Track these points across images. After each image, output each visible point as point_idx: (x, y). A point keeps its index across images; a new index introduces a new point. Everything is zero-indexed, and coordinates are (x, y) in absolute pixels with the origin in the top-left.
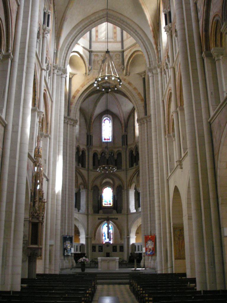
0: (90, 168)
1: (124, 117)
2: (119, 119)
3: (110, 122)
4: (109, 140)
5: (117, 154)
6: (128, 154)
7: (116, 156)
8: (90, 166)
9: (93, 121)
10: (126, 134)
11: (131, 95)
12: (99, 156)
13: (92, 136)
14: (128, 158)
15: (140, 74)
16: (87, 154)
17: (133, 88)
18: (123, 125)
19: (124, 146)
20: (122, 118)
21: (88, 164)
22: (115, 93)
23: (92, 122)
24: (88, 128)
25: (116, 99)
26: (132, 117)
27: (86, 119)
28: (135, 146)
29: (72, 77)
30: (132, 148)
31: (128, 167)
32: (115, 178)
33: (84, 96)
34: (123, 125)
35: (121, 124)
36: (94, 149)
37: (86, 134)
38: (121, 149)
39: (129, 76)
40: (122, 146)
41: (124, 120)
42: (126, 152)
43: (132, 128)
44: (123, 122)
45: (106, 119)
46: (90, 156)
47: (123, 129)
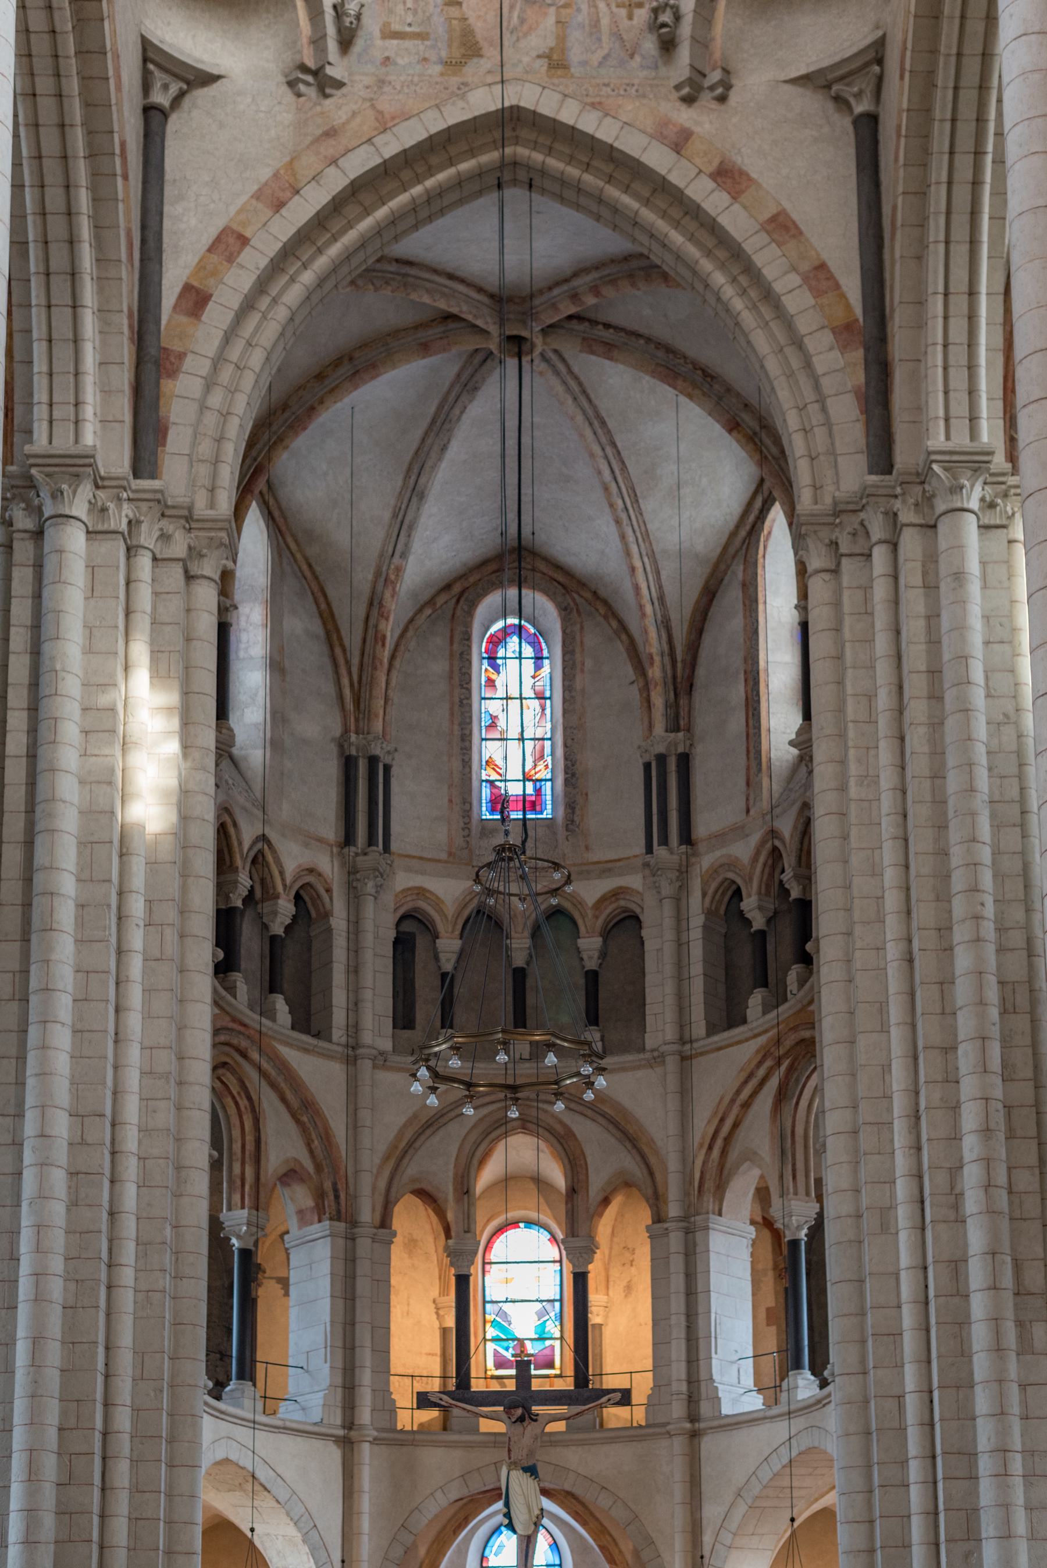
1: (662, 598)
3: (538, 659)
4: (531, 804)
7: (597, 942)
8: (368, 1021)
9: (390, 629)
10: (681, 749)
13: (387, 768)
14: (697, 950)
15: (828, 87)
16: (339, 922)
18: (655, 672)
19: (659, 851)
20: (649, 609)
22: (590, 345)
23: (390, 643)
24: (347, 692)
25: (597, 420)
26: (731, 596)
27: (328, 618)
28: (762, 843)
30: (731, 864)
31: (699, 1028)
32: (587, 1131)
33: (294, 295)
34: (655, 672)
35: (639, 663)
36: (403, 880)
37: (334, 749)
38: (634, 881)
39: (722, 99)
40: (649, 849)
41: (665, 624)
43: (738, 692)
44: (653, 644)
45: (506, 632)
46: (368, 939)
47: (658, 701)
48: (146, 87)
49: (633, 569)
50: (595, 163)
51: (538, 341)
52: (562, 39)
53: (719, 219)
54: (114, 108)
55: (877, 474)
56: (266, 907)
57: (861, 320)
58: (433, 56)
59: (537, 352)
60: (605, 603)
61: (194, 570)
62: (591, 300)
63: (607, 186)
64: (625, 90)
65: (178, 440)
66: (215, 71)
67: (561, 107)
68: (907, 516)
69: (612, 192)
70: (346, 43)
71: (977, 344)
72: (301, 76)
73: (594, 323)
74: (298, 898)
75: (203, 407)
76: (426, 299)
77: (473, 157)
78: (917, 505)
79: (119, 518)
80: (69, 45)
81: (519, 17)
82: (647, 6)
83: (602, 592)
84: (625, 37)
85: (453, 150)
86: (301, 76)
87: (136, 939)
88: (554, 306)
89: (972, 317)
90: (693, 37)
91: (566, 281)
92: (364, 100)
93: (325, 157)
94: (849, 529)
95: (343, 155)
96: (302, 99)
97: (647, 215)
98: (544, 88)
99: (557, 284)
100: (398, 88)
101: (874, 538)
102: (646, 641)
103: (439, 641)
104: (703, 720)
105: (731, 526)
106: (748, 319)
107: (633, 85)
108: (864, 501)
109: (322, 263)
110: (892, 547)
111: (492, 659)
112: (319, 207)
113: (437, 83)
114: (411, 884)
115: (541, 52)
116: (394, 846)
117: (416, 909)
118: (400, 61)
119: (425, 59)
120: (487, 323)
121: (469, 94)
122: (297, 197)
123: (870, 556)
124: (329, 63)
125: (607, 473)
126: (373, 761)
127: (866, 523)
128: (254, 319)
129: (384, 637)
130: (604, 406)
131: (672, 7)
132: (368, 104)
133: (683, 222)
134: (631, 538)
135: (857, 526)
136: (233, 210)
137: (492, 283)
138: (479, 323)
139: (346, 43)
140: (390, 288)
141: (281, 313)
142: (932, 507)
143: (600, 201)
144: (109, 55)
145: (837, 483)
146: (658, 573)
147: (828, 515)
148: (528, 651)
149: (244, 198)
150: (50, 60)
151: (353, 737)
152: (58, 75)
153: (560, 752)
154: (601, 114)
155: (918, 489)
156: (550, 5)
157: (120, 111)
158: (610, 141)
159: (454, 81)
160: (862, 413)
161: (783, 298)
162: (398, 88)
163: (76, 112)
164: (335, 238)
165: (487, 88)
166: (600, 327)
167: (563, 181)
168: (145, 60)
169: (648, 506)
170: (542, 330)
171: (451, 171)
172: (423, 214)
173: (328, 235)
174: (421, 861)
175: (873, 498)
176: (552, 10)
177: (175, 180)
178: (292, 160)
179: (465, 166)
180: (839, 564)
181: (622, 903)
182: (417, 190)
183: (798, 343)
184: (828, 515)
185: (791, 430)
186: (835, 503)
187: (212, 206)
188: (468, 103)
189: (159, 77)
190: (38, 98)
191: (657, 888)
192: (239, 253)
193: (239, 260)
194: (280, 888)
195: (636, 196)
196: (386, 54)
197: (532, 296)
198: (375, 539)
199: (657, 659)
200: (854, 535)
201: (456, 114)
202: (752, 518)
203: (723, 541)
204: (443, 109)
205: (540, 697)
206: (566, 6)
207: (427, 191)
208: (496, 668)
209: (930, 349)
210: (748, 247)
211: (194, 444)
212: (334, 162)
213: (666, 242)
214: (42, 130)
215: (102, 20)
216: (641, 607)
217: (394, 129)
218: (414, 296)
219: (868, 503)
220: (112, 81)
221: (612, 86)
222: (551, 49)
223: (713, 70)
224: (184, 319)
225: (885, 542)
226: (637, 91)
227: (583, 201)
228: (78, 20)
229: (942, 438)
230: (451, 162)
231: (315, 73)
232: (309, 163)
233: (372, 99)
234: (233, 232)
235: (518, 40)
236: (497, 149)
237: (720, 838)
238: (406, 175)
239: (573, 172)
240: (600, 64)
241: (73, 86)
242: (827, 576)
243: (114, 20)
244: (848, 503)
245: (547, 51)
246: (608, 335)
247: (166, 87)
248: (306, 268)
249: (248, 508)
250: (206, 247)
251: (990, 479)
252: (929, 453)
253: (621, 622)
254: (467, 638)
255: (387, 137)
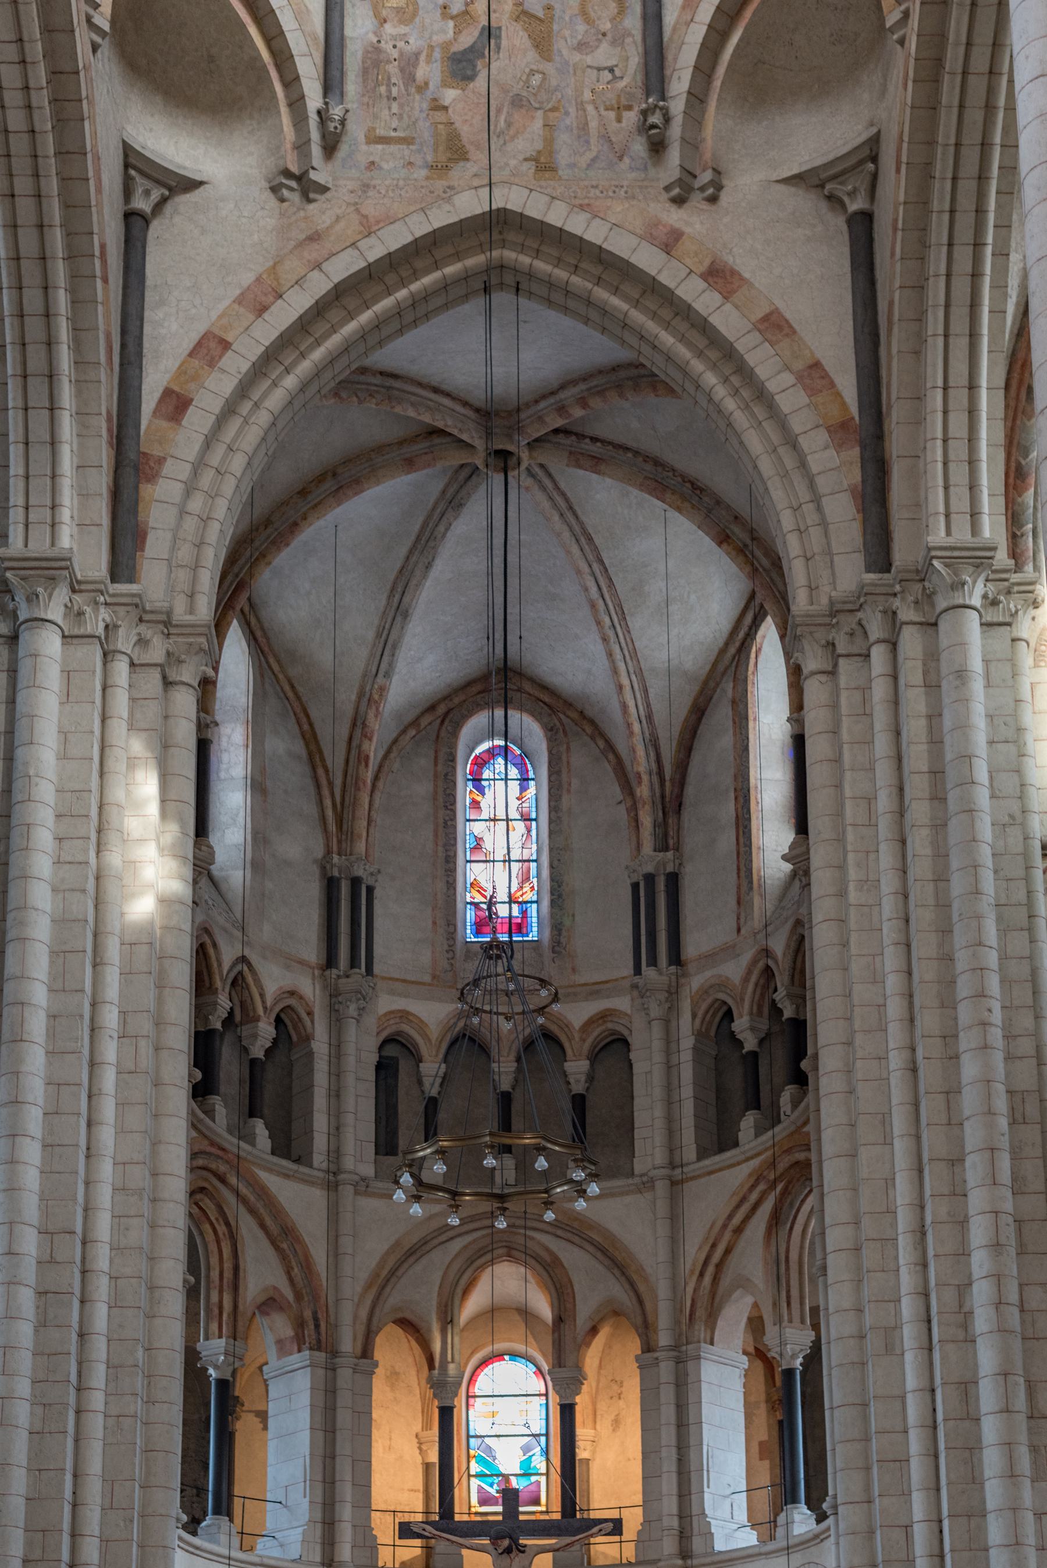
0: (349, 1163)
1: (650, 717)
2: (610, 747)
3: (524, 780)
4: (517, 927)
5: (587, 1046)
6: (687, 1042)
10: (670, 869)
11: (736, 393)
12: (432, 1068)
13: (370, 890)
16: (320, 1045)
17: (760, 314)
18: (643, 791)
19: (649, 972)
20: (636, 727)
21: (336, 1130)
22: (577, 459)
24: (329, 813)
25: (584, 537)
26: (721, 714)
29: (159, 207)
30: (722, 984)
33: (276, 399)
34: (643, 791)
36: (386, 1003)
37: (316, 870)
40: (638, 971)
41: (654, 743)
42: (667, 1023)
43: (729, 810)
44: (641, 762)
45: (491, 753)
46: (350, 1062)
47: (647, 820)
48: (128, 193)
49: (620, 687)
50: (583, 265)
51: (525, 455)
52: (549, 142)
53: (711, 319)
54: (94, 209)
55: (875, 572)
56: (245, 1031)
57: (857, 418)
58: (418, 160)
59: (523, 466)
60: (592, 722)
61: (173, 676)
62: (578, 413)
63: (596, 288)
64: (614, 192)
65: (156, 545)
66: (198, 178)
67: (548, 209)
68: (907, 613)
69: (601, 294)
70: (330, 148)
71: (978, 439)
72: (284, 181)
73: (581, 436)
74: (279, 1021)
75: (183, 512)
76: (411, 413)
77: (459, 260)
78: (916, 603)
79: (96, 622)
80: (48, 145)
81: (505, 121)
82: (636, 109)
83: (589, 713)
84: (614, 139)
85: (438, 254)
86: (284, 181)
87: (110, 1051)
88: (541, 419)
89: (972, 412)
90: (683, 139)
91: (552, 393)
92: (348, 204)
93: (309, 261)
94: (847, 629)
95: (327, 259)
96: (285, 204)
97: (637, 317)
98: (531, 190)
99: (544, 397)
100: (383, 192)
101: (873, 638)
102: (634, 760)
103: (423, 762)
104: (693, 838)
105: (721, 643)
106: (740, 419)
107: (622, 187)
108: (862, 600)
109: (305, 367)
110: (891, 646)
111: (477, 781)
112: (301, 312)
113: (422, 187)
114: (395, 1007)
115: (528, 155)
116: (377, 969)
117: (400, 1033)
118: (385, 166)
119: (410, 163)
120: (473, 437)
121: (455, 197)
122: (280, 301)
123: (868, 656)
124: (313, 168)
125: (594, 590)
126: (356, 882)
127: (864, 623)
128: (235, 424)
129: (367, 757)
130: (591, 521)
131: (661, 109)
132: (353, 208)
133: (673, 323)
134: (618, 656)
135: (854, 626)
136: (214, 314)
137: (478, 397)
138: (464, 437)
139: (330, 148)
140: (374, 400)
141: (263, 418)
142: (933, 605)
143: (589, 303)
144: (89, 156)
145: (834, 584)
146: (646, 691)
147: (824, 616)
148: (514, 772)
149: (226, 303)
150: (29, 160)
151: (336, 858)
152: (36, 175)
153: (546, 873)
154: (589, 216)
155: (919, 586)
156: (536, 109)
157: (100, 213)
158: (598, 243)
159: (440, 184)
160: (858, 512)
161: (776, 397)
162: (383, 192)
163: (55, 211)
164: (318, 343)
165: (473, 191)
166: (587, 440)
167: (551, 284)
168: (127, 166)
169: (636, 623)
170: (528, 444)
171: (436, 275)
172: (408, 318)
173: (312, 339)
174: (405, 985)
175: (869, 597)
176: (540, 113)
177: (156, 286)
178: (275, 264)
179: (450, 270)
180: (836, 665)
181: (610, 1025)
182: (402, 294)
183: (793, 443)
184: (824, 616)
185: (785, 530)
186: (832, 603)
187: (194, 311)
188: (454, 206)
189: (141, 183)
190: (17, 199)
191: (646, 1010)
192: (220, 357)
193: (220, 364)
194: (260, 1011)
195: (626, 298)
196: (371, 159)
197: (519, 410)
198: (359, 658)
199: (645, 778)
200: (851, 634)
201: (441, 218)
202: (741, 635)
203: (712, 658)
204: (428, 212)
205: (526, 818)
206: (554, 109)
207: (412, 294)
208: (481, 791)
209: (929, 445)
210: (740, 347)
211: (174, 548)
212: (318, 266)
213: (656, 343)
214: (20, 231)
215: (83, 120)
216: (629, 725)
217: (379, 233)
218: (398, 410)
219: (865, 602)
220: (92, 182)
221: (601, 188)
222: (539, 152)
223: (704, 171)
224: (164, 424)
225: (884, 641)
226: (626, 192)
227: (571, 304)
228: (58, 120)
229: (943, 533)
230: (437, 266)
231: (299, 178)
232: (293, 267)
233: (356, 203)
234: (215, 336)
235: (505, 144)
236: (483, 252)
237: (711, 958)
238: (391, 278)
239: (561, 274)
240: (589, 166)
241: (52, 186)
242: (823, 678)
243: (94, 122)
244: (845, 602)
245: (534, 154)
246: (596, 449)
247: (147, 193)
248: (289, 373)
249: (229, 624)
250: (187, 352)
251: (991, 577)
252: (929, 549)
253: (608, 742)
254: (452, 759)
255: (372, 240)
